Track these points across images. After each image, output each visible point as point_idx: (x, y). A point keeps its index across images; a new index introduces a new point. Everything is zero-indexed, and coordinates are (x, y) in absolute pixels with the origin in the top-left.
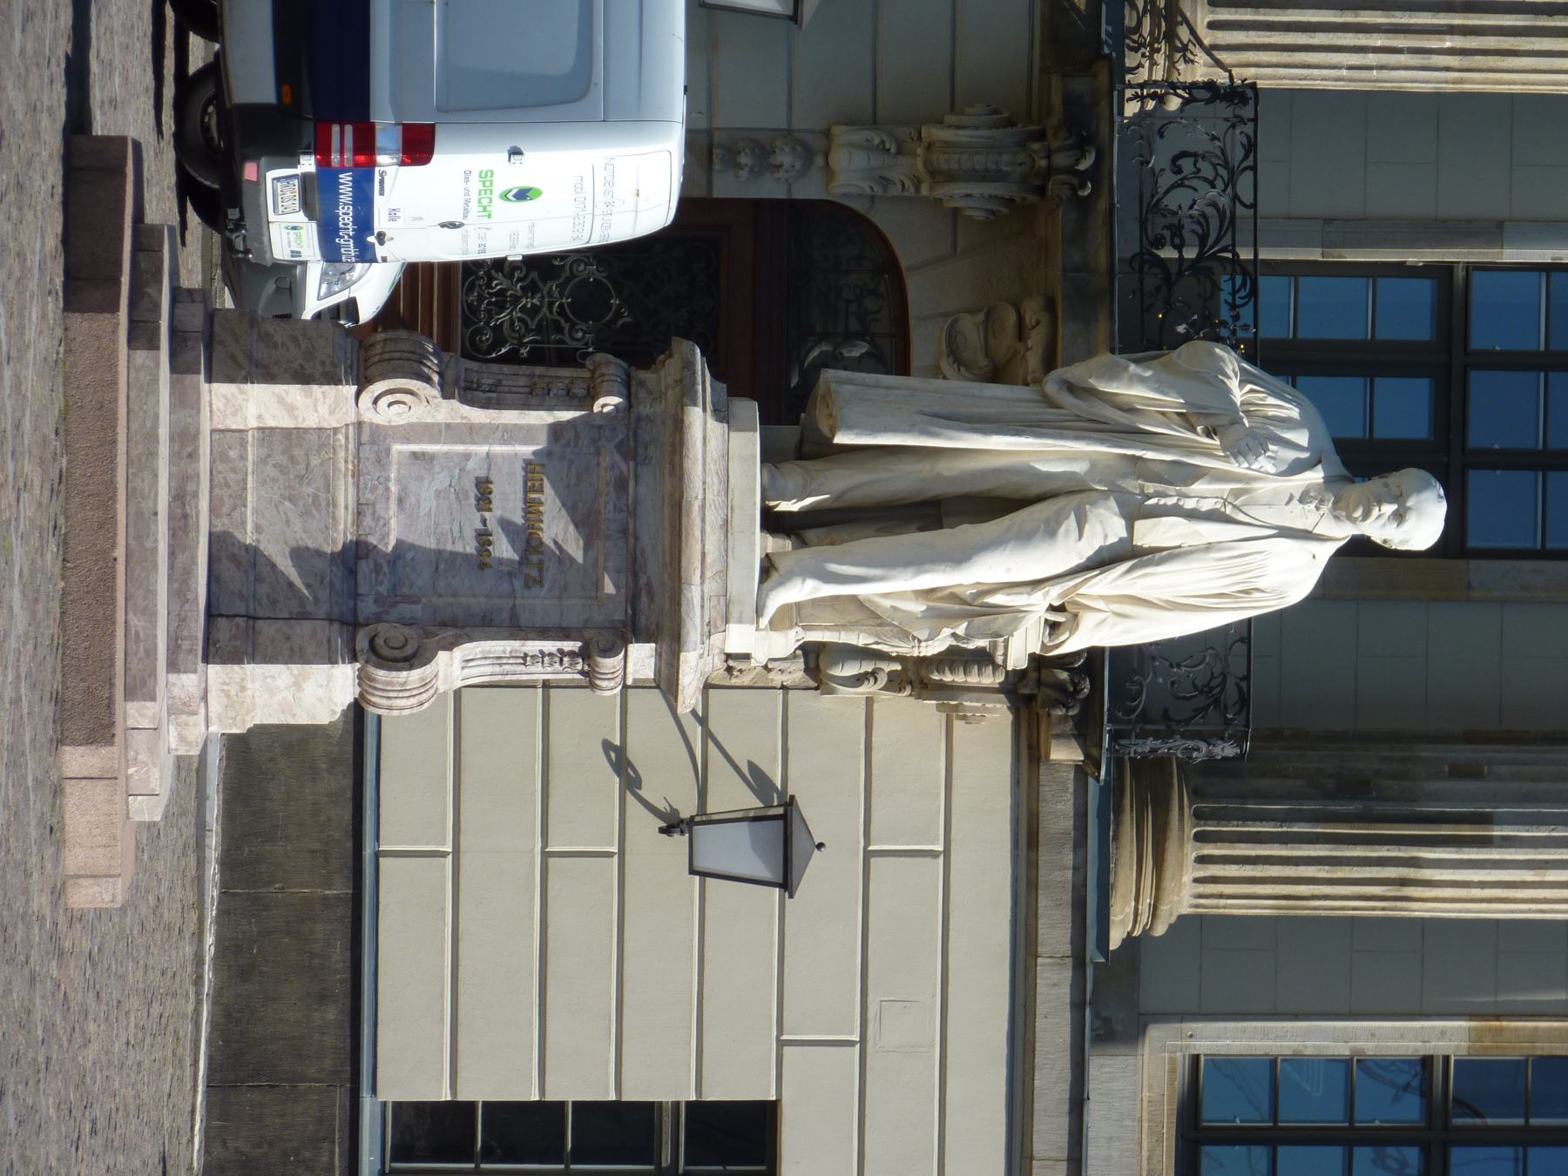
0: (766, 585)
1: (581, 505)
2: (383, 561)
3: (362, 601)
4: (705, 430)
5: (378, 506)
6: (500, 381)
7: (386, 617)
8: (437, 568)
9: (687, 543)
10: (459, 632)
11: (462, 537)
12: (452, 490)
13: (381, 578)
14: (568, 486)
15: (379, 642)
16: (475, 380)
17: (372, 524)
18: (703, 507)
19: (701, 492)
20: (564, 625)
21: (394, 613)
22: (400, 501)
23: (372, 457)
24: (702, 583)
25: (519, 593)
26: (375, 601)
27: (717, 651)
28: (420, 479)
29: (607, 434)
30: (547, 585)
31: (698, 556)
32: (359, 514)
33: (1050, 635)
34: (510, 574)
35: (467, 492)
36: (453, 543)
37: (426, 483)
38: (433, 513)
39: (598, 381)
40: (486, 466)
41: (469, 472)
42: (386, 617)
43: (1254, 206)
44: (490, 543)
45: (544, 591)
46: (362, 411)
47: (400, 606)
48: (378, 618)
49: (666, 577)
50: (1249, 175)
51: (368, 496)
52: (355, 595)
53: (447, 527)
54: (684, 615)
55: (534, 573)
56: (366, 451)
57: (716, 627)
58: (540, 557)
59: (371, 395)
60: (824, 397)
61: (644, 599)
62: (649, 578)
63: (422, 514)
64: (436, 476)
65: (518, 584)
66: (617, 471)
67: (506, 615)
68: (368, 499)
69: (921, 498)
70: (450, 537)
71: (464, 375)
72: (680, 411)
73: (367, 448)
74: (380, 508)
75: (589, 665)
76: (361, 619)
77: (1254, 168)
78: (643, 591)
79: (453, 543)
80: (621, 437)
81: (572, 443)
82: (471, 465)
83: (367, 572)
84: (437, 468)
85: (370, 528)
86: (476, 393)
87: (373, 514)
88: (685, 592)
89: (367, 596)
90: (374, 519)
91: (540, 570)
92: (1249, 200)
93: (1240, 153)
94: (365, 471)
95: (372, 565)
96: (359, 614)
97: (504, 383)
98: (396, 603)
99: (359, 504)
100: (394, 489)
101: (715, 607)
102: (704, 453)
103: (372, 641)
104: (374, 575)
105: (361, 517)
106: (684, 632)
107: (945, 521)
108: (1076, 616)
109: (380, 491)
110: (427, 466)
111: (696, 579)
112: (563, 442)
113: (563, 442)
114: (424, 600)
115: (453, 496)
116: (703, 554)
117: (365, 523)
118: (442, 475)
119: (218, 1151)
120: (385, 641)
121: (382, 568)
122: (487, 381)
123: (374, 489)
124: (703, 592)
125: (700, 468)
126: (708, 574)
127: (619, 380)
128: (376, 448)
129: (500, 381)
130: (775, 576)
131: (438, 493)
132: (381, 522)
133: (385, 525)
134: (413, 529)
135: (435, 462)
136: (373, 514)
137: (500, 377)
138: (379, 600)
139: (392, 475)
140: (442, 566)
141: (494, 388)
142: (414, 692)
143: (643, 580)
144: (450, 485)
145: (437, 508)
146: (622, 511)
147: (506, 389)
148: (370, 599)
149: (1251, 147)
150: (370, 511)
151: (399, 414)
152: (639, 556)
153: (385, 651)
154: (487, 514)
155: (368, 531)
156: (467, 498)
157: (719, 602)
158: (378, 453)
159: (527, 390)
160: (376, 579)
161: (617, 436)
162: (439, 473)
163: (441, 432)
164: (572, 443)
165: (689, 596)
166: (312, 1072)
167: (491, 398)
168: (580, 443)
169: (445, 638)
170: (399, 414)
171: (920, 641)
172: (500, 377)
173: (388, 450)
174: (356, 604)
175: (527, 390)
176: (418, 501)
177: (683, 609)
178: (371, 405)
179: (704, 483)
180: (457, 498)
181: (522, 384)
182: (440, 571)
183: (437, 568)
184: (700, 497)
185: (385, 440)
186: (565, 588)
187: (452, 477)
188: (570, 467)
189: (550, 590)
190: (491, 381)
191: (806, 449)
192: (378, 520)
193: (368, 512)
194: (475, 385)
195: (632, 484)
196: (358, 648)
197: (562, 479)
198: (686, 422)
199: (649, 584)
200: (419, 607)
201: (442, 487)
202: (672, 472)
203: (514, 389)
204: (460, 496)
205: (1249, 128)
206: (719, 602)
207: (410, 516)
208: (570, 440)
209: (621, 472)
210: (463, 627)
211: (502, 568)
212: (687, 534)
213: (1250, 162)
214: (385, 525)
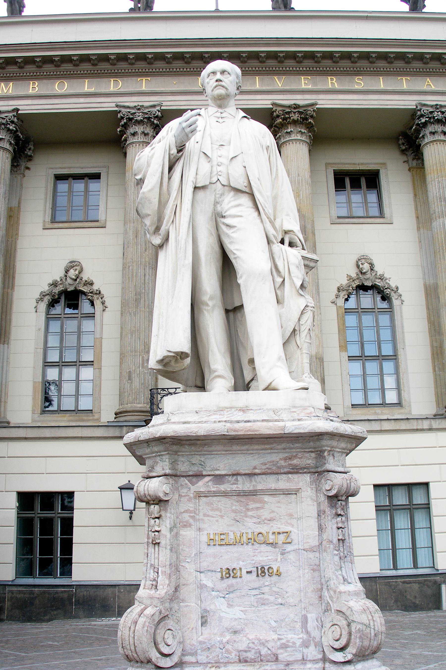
0: (279, 387)
1: (234, 507)
2: (278, 643)
3: (307, 656)
4: (179, 423)
5: (241, 648)
6: (151, 565)
7: (318, 639)
8: (281, 604)
9: (257, 431)
10: (325, 587)
11: (259, 588)
12: (227, 596)
13: (290, 644)
14: (222, 517)
15: (337, 645)
16: (151, 582)
17: (253, 651)
18: (231, 422)
19: (221, 423)
20: (316, 515)
21: (315, 633)
22: (235, 632)
23: (206, 653)
24: (283, 421)
25: (296, 547)
26: (307, 647)
27: (325, 413)
28: (220, 618)
29: (185, 490)
30: (288, 529)
31: (265, 424)
32: (246, 661)
33: (297, 247)
34: (282, 554)
35: (228, 586)
36: (263, 593)
37: (222, 614)
38: (243, 609)
39: (149, 498)
40: (209, 573)
41: (215, 586)
42: (318, 639)
43: (176, 388)
44: (263, 567)
45: (294, 530)
46: (173, 664)
47: (309, 629)
48: (319, 645)
49: (279, 447)
50: (169, 390)
51: (233, 655)
52: (304, 661)
53: (253, 598)
54: (306, 431)
55: (282, 538)
56: (202, 658)
57: (311, 413)
58: (271, 534)
59: (159, 660)
60: (165, 366)
61: (295, 462)
62: (281, 459)
63: (243, 616)
64: (219, 608)
65: (289, 548)
66: (210, 484)
67: (311, 555)
68: (236, 655)
69: (227, 324)
70: (259, 596)
71: (148, 591)
72: (166, 440)
73: (199, 658)
74: (242, 646)
75: (342, 496)
76: (320, 656)
77: (168, 389)
78: (290, 462)
79: (263, 593)
80: (187, 482)
81: (192, 515)
82: (210, 584)
83: (286, 654)
84: (212, 607)
85: (256, 653)
86: (159, 582)
87: (246, 651)
88: (290, 431)
89: (303, 653)
90: (250, 651)
91: (279, 533)
92: (175, 389)
93: (165, 392)
94: (216, 659)
95: (281, 651)
96: (316, 658)
97: (153, 563)
98: (307, 632)
99: (240, 661)
100: (228, 637)
101: (298, 414)
102: (194, 422)
103: (336, 650)
104: (288, 649)
105: (249, 660)
106: (318, 431)
107: (237, 304)
108: (286, 232)
109: (229, 647)
110: (212, 614)
111: (281, 424)
112: (191, 521)
113: (191, 521)
114: (303, 613)
115: (231, 595)
116: (263, 421)
117: (253, 657)
118: (217, 604)
119: (394, 608)
120: (337, 640)
121: (284, 644)
122: (152, 575)
123: (228, 651)
124: (288, 420)
125: (204, 425)
126: (276, 418)
127: (147, 484)
128: (199, 651)
129: (151, 565)
130: (273, 385)
131: (230, 606)
132: (251, 645)
133: (253, 643)
134: (255, 622)
135: (208, 609)
136: (246, 651)
137: (149, 565)
138: (306, 645)
139: (219, 639)
140: (280, 601)
141: (156, 570)
142: (370, 617)
143: (282, 463)
144: (224, 598)
145: (240, 606)
146: (237, 480)
147: (157, 561)
148: (305, 650)
149: (163, 389)
150: (244, 654)
151: (174, 637)
152: (267, 466)
153: (343, 642)
154: (244, 571)
155: (258, 655)
156: (232, 585)
157: (295, 412)
158: (203, 650)
159: (157, 546)
160: (292, 647)
161: (186, 484)
162: (216, 606)
163: (187, 606)
164: (192, 515)
165: (293, 428)
166: (375, 587)
167: (162, 572)
168: (191, 509)
169: (330, 597)
170: (173, 638)
171: (307, 306)
172: (149, 565)
173: (201, 643)
174: (310, 661)
175: (157, 546)
176: (236, 619)
177: (302, 431)
178: (168, 659)
179: (215, 422)
180: (232, 592)
181: (153, 550)
182: (283, 602)
183: (281, 604)
184: (224, 424)
185: (194, 645)
186: (290, 515)
187: (217, 597)
188: (208, 516)
189: (293, 526)
190: (152, 571)
191: (199, 384)
192: (250, 648)
193: (244, 655)
194: (154, 583)
195: (217, 472)
196: (343, 660)
197: (217, 521)
198: (172, 434)
199: (285, 459)
200: (309, 616)
201: (226, 603)
202: (209, 445)
203: (156, 555)
204: (230, 591)
205: (159, 390)
206: (295, 412)
207: (246, 624)
208: (190, 516)
209: (211, 480)
210: (322, 584)
211: (279, 559)
212: (249, 430)
213: (166, 390)
214: (253, 643)
